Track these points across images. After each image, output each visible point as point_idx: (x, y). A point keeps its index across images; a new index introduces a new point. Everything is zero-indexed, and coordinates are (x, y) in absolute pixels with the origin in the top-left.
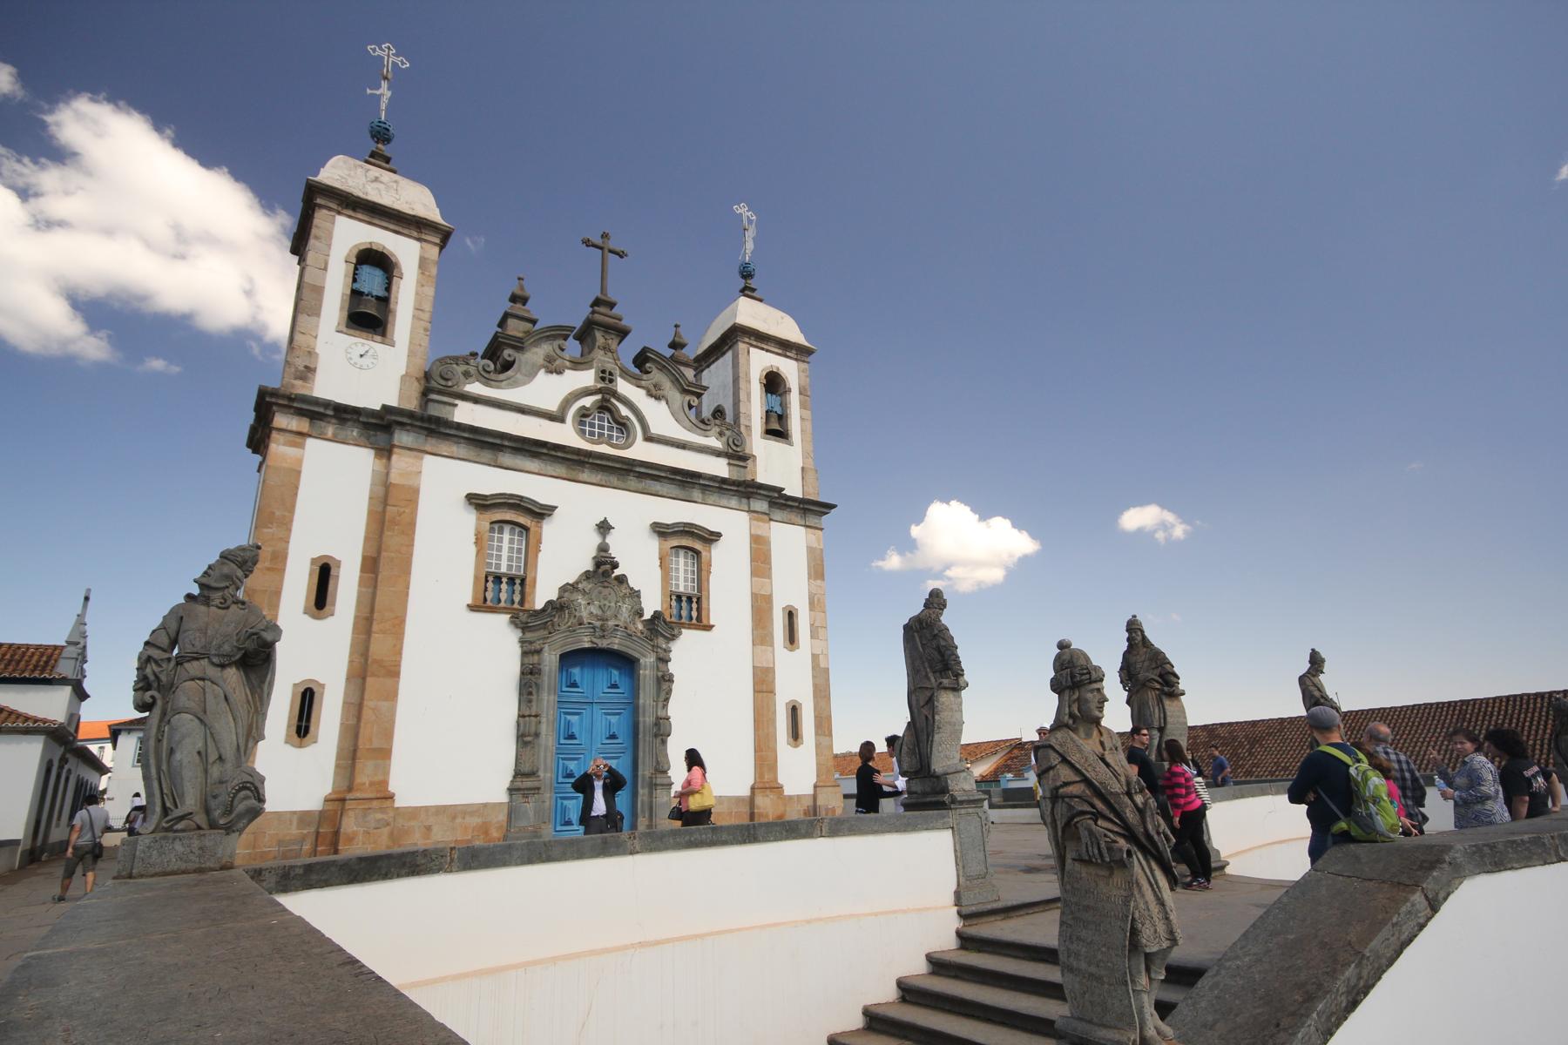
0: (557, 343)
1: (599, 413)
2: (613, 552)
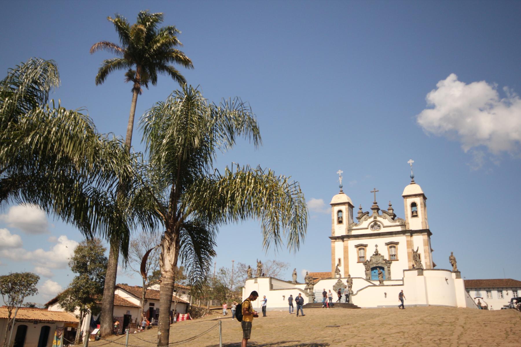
0: (366, 215)
2: (378, 250)
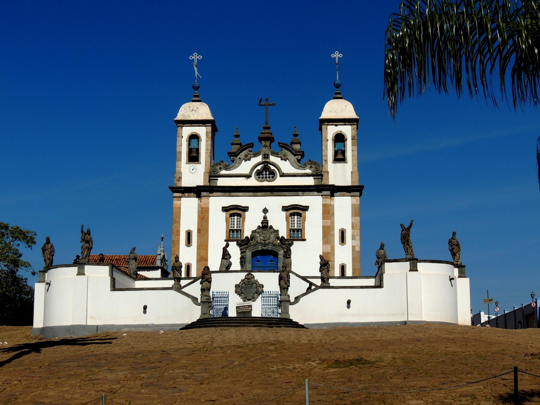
0: (248, 150)
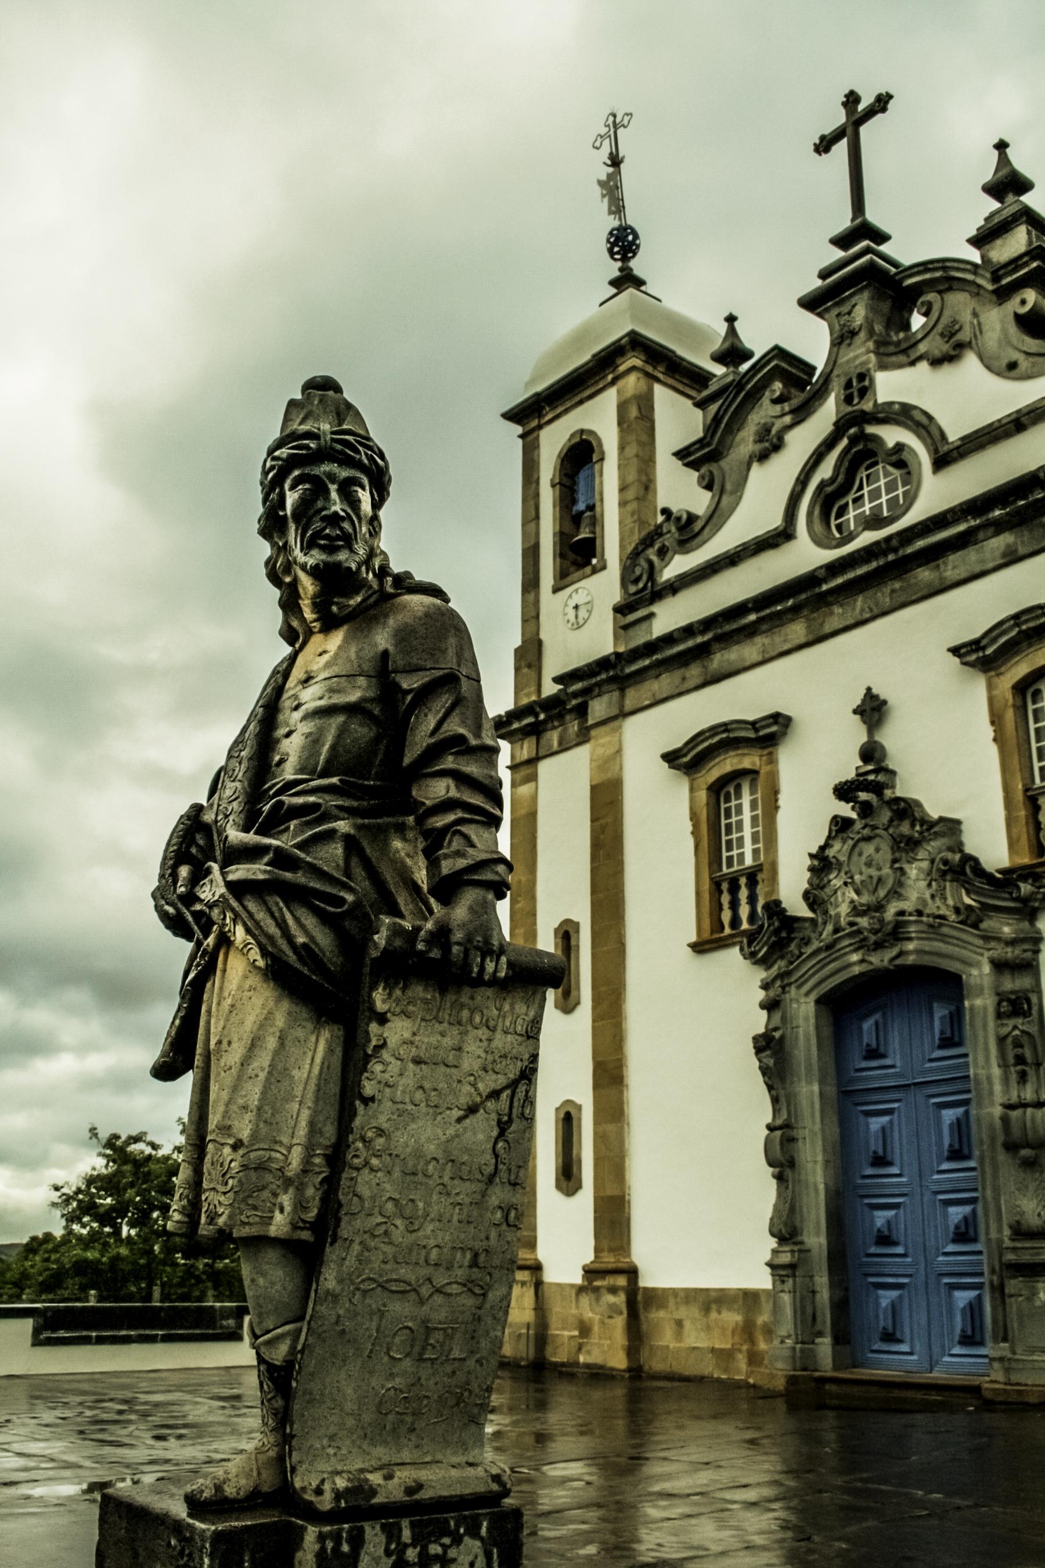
0: (766, 401)
1: (867, 469)
